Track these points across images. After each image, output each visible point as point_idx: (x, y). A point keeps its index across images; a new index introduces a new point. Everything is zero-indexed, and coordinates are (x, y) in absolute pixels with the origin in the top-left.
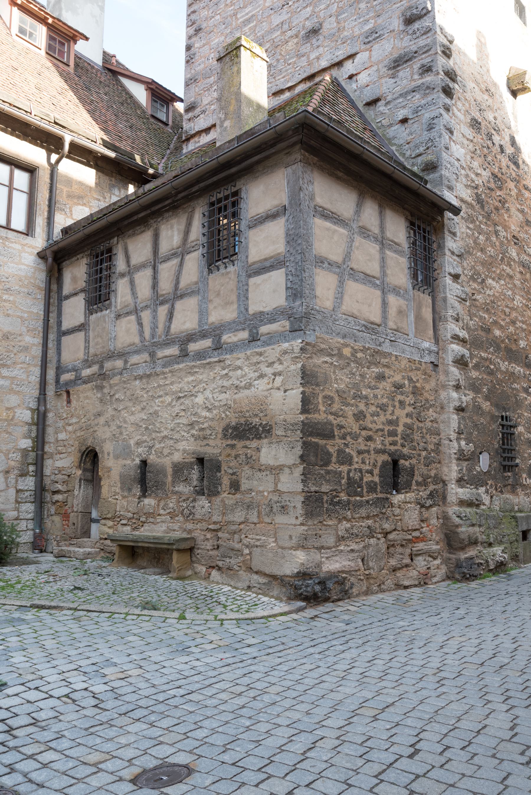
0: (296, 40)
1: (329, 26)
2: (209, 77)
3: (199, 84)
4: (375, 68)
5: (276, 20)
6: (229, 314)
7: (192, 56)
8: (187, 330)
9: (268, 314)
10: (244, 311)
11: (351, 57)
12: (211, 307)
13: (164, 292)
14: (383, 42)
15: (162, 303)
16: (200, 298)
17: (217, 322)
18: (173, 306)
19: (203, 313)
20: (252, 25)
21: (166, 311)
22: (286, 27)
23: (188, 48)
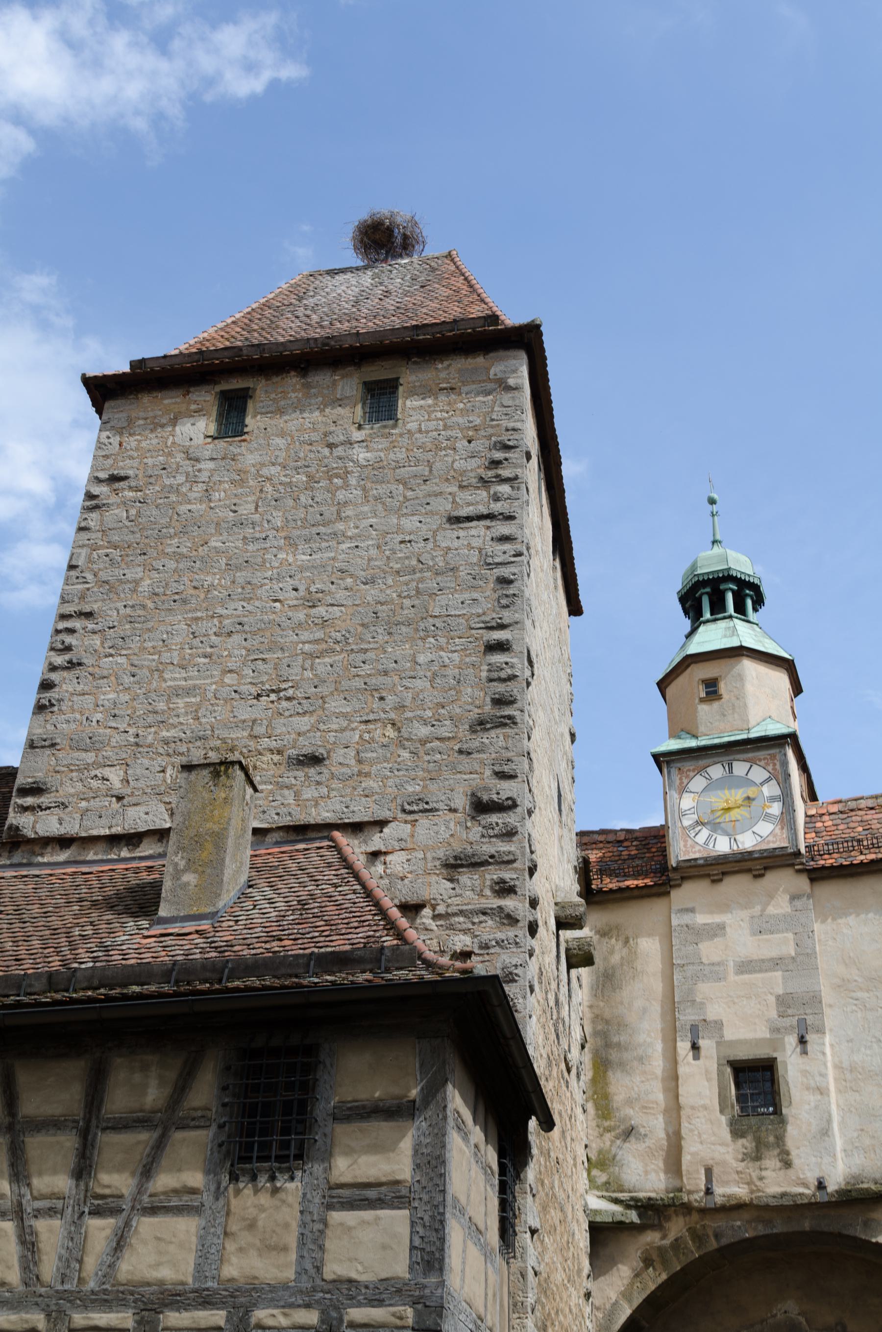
0: (278, 757)
1: (342, 759)
2: (86, 751)
3: (60, 754)
4: (420, 855)
5: (245, 713)
6: (279, 1269)
7: (53, 701)
8: (161, 1283)
9: (367, 1287)
10: (312, 1272)
11: (381, 824)
12: (231, 1246)
13: (107, 1191)
14: (436, 820)
15: (97, 1212)
16: (203, 1223)
17: (242, 1280)
18: (127, 1224)
19: (207, 1255)
20: (193, 700)
21: (108, 1232)
22: (260, 730)
23: (46, 686)
